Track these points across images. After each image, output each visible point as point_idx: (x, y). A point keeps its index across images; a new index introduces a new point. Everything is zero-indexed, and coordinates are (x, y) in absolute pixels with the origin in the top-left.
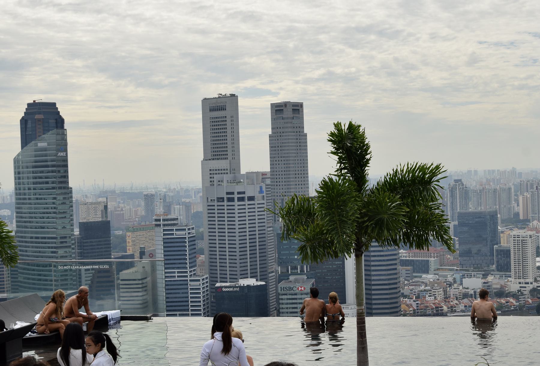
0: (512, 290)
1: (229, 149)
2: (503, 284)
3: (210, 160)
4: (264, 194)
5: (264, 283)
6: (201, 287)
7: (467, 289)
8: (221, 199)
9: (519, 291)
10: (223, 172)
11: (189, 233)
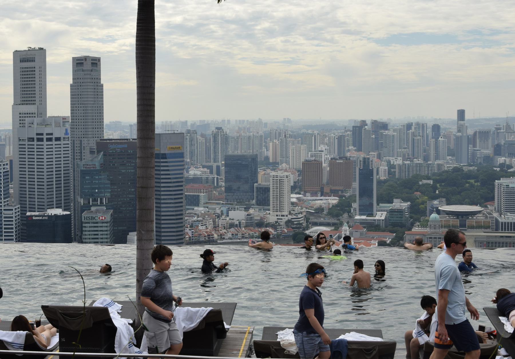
0: (270, 222)
1: (37, 96)
2: (262, 216)
3: (19, 104)
4: (69, 136)
5: (69, 213)
6: (14, 216)
7: (233, 220)
8: (31, 139)
9: (276, 222)
10: (31, 115)
11: (4, 168)
